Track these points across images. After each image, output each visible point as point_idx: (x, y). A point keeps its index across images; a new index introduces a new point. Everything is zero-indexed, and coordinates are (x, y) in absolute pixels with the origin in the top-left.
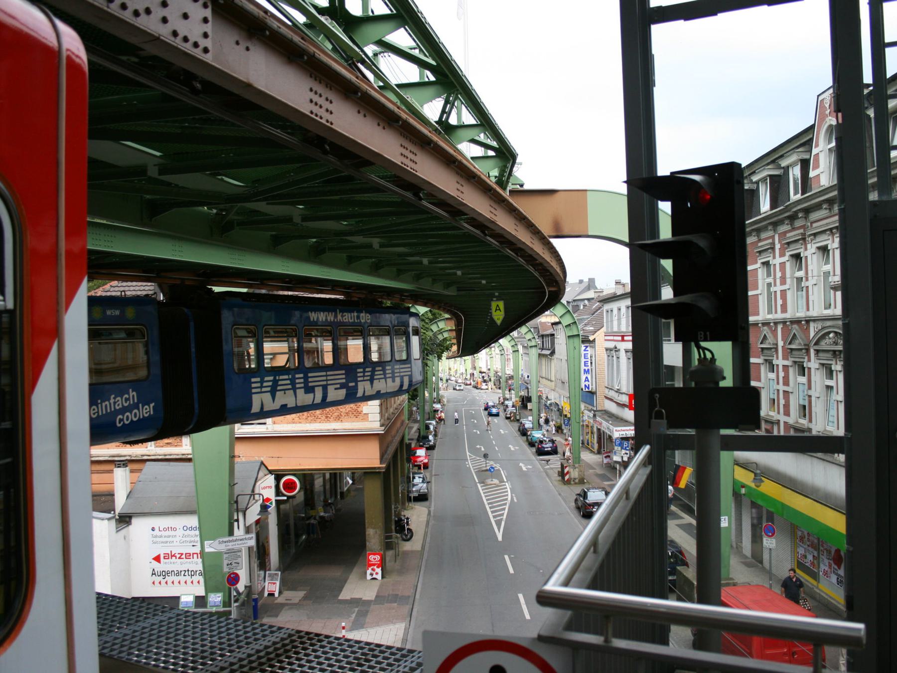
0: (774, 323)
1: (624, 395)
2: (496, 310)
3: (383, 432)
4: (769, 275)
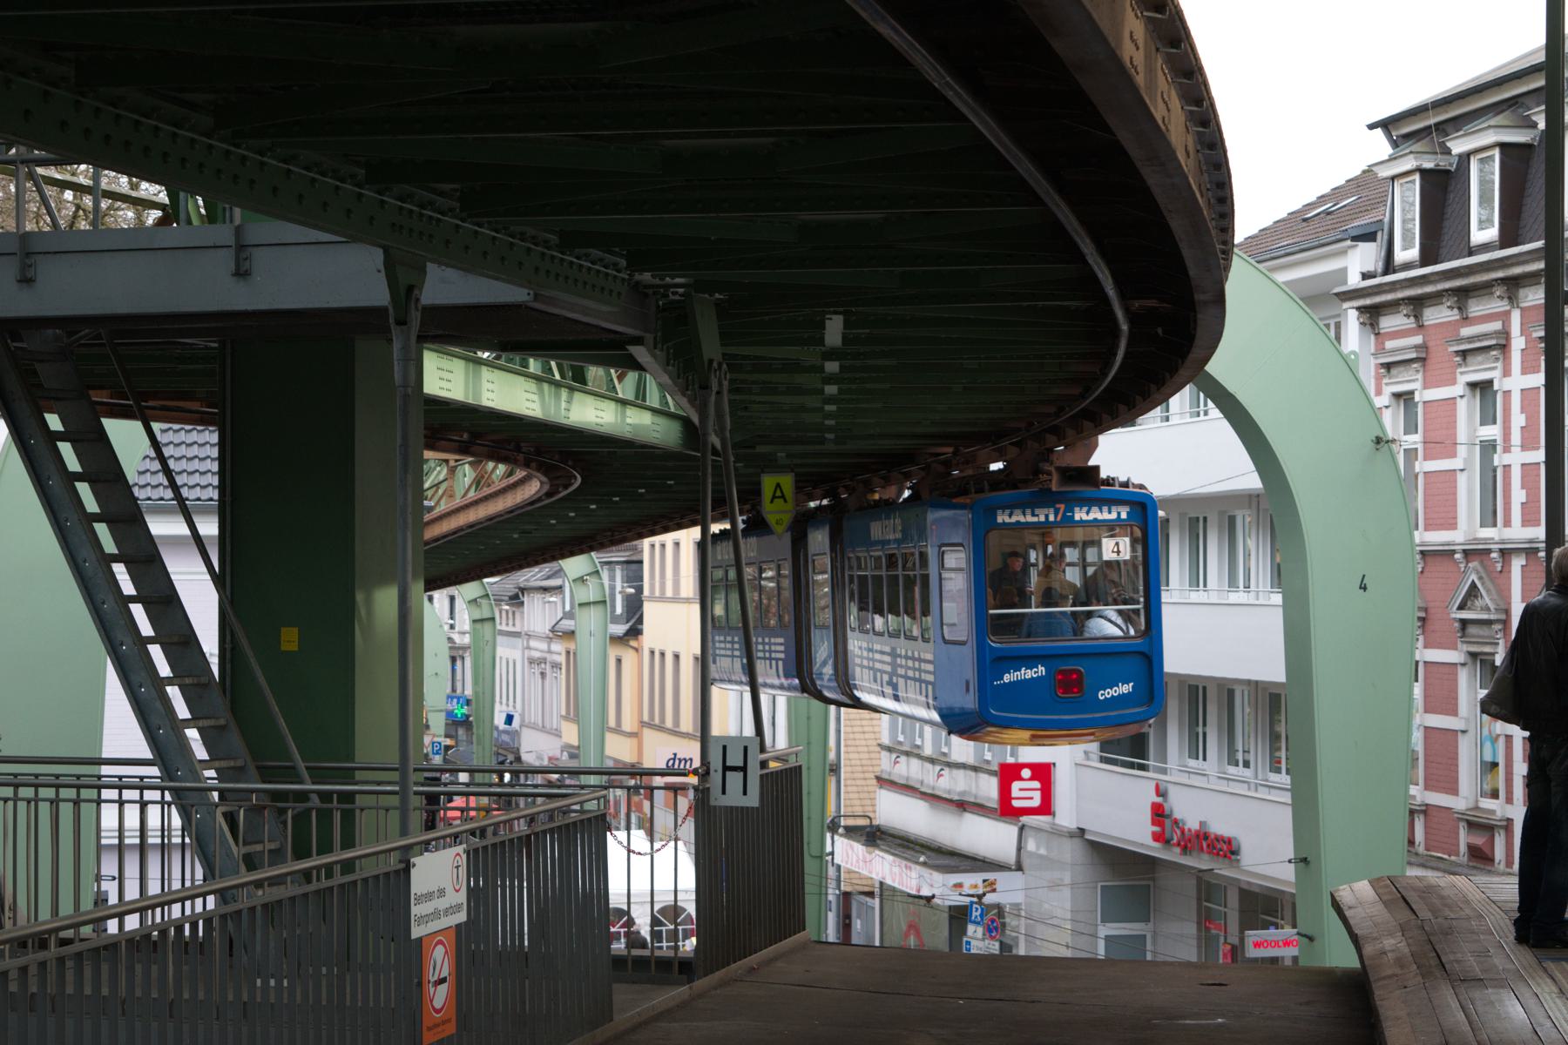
0: (1502, 551)
1: (960, 773)
4: (1488, 418)
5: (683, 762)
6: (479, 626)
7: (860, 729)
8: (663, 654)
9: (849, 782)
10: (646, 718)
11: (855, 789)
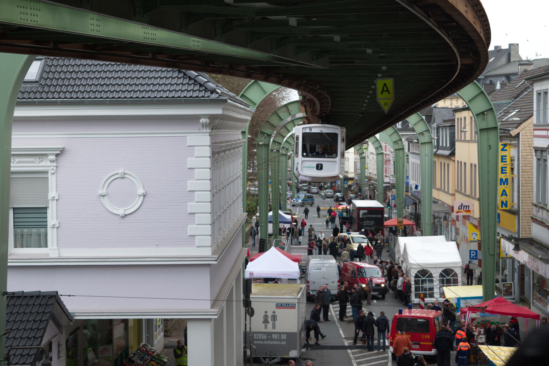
2: (383, 91)
3: (216, 263)
5: (465, 207)
6: (397, 152)
7: (528, 196)
8: (461, 163)
9: (523, 218)
10: (456, 189)
11: (526, 221)
